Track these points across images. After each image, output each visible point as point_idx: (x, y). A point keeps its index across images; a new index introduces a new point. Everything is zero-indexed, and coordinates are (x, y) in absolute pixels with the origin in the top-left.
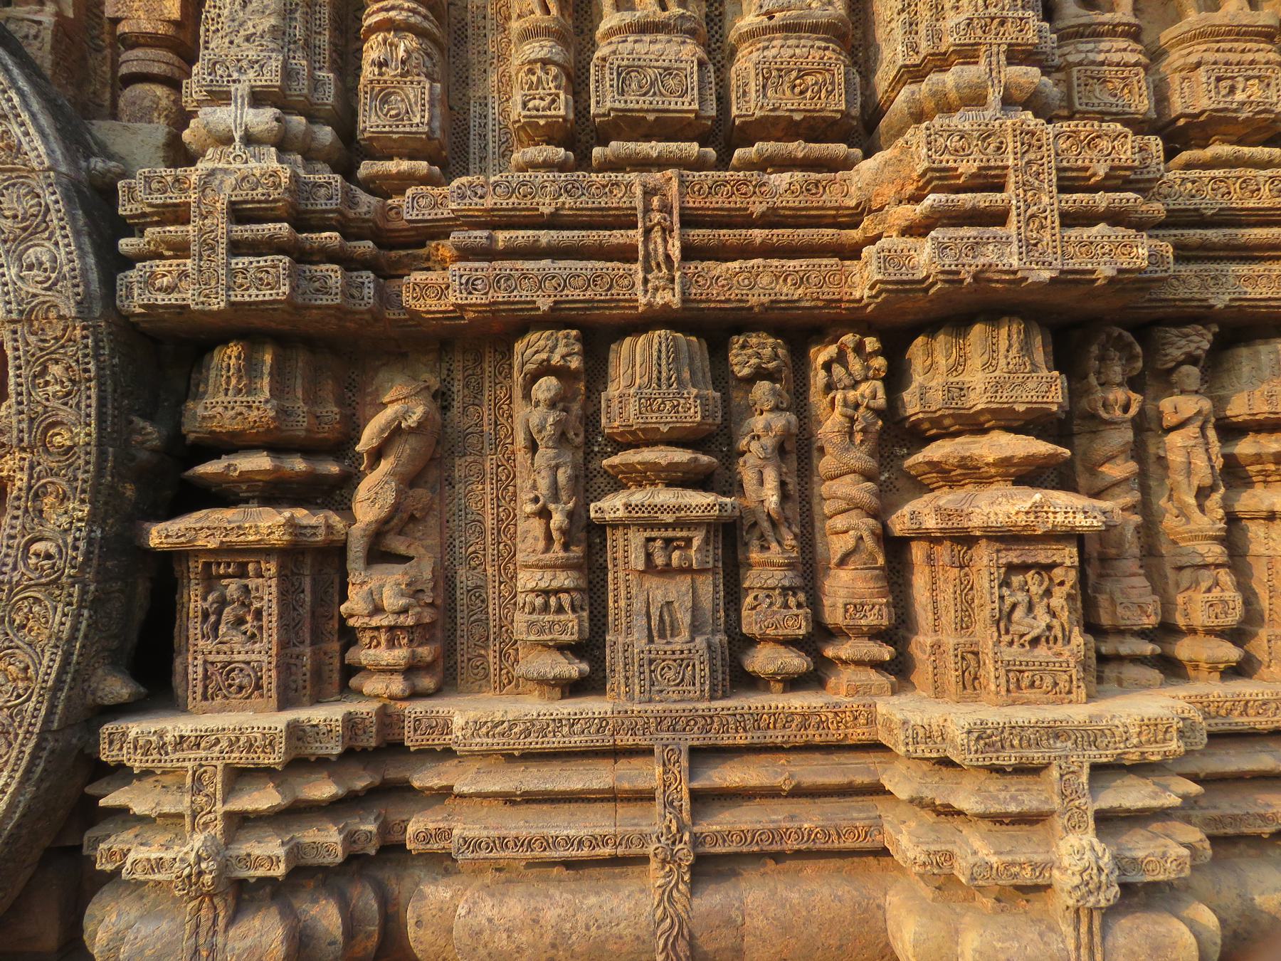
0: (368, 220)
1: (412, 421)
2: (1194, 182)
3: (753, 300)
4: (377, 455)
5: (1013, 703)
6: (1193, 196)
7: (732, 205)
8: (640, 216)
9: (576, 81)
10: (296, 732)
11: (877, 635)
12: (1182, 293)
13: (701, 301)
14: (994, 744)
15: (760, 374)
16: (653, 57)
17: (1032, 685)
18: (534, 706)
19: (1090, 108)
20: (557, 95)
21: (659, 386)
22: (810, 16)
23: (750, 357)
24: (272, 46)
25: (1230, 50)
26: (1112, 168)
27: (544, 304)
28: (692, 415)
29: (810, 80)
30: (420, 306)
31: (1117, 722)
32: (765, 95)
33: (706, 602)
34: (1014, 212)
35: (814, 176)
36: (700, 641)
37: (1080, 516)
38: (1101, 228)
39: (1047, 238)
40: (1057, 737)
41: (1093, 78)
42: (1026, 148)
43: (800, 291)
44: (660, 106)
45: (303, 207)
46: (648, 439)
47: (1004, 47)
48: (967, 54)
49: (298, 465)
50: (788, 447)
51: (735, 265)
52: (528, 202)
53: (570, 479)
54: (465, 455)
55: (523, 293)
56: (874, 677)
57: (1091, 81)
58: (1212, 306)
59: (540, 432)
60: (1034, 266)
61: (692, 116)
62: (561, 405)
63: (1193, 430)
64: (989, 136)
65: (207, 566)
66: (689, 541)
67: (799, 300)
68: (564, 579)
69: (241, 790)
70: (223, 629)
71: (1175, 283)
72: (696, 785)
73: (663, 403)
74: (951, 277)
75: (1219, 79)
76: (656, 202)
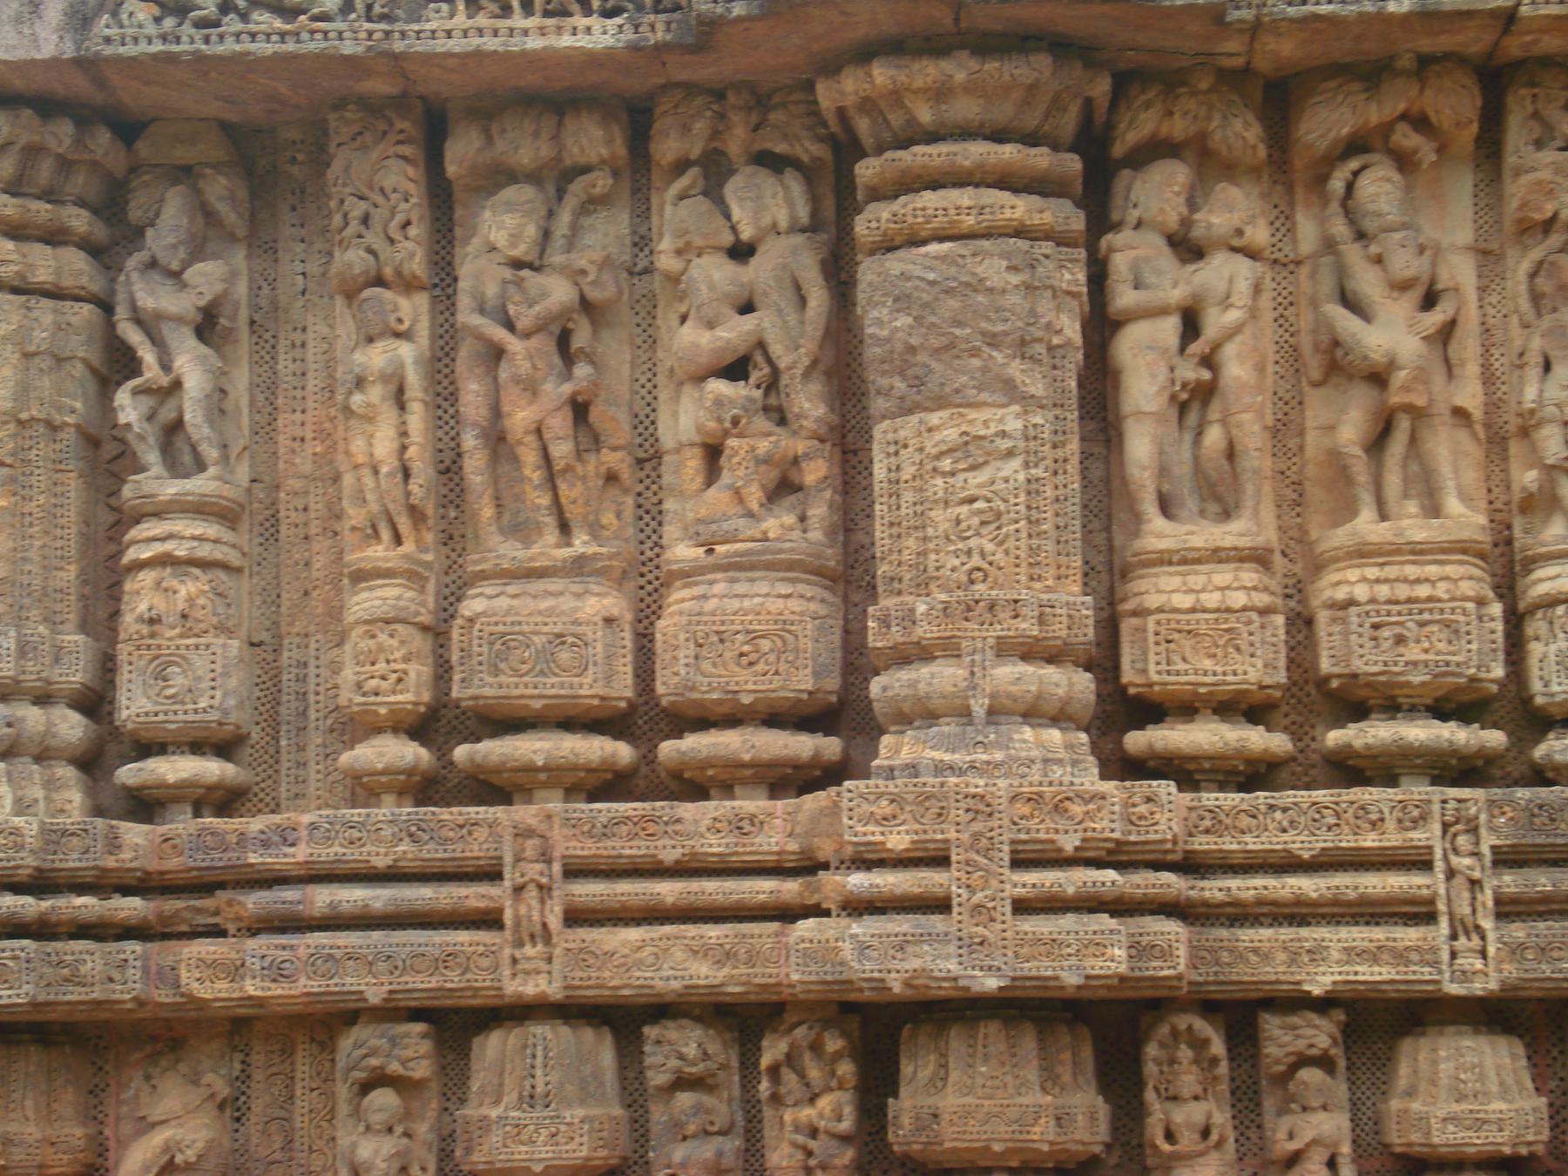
2: (1285, 810)
6: (1284, 831)
7: (634, 852)
12: (1267, 972)
20: (405, 672)
23: (667, 1057)
26: (1084, 840)
29: (765, 645)
30: (203, 992)
34: (955, 901)
38: (1068, 921)
41: (1179, 631)
42: (971, 815)
47: (991, 641)
48: (949, 649)
57: (1176, 636)
58: (1309, 992)
60: (977, 973)
64: (927, 798)
71: (1253, 958)
73: (536, 1131)
74: (874, 984)
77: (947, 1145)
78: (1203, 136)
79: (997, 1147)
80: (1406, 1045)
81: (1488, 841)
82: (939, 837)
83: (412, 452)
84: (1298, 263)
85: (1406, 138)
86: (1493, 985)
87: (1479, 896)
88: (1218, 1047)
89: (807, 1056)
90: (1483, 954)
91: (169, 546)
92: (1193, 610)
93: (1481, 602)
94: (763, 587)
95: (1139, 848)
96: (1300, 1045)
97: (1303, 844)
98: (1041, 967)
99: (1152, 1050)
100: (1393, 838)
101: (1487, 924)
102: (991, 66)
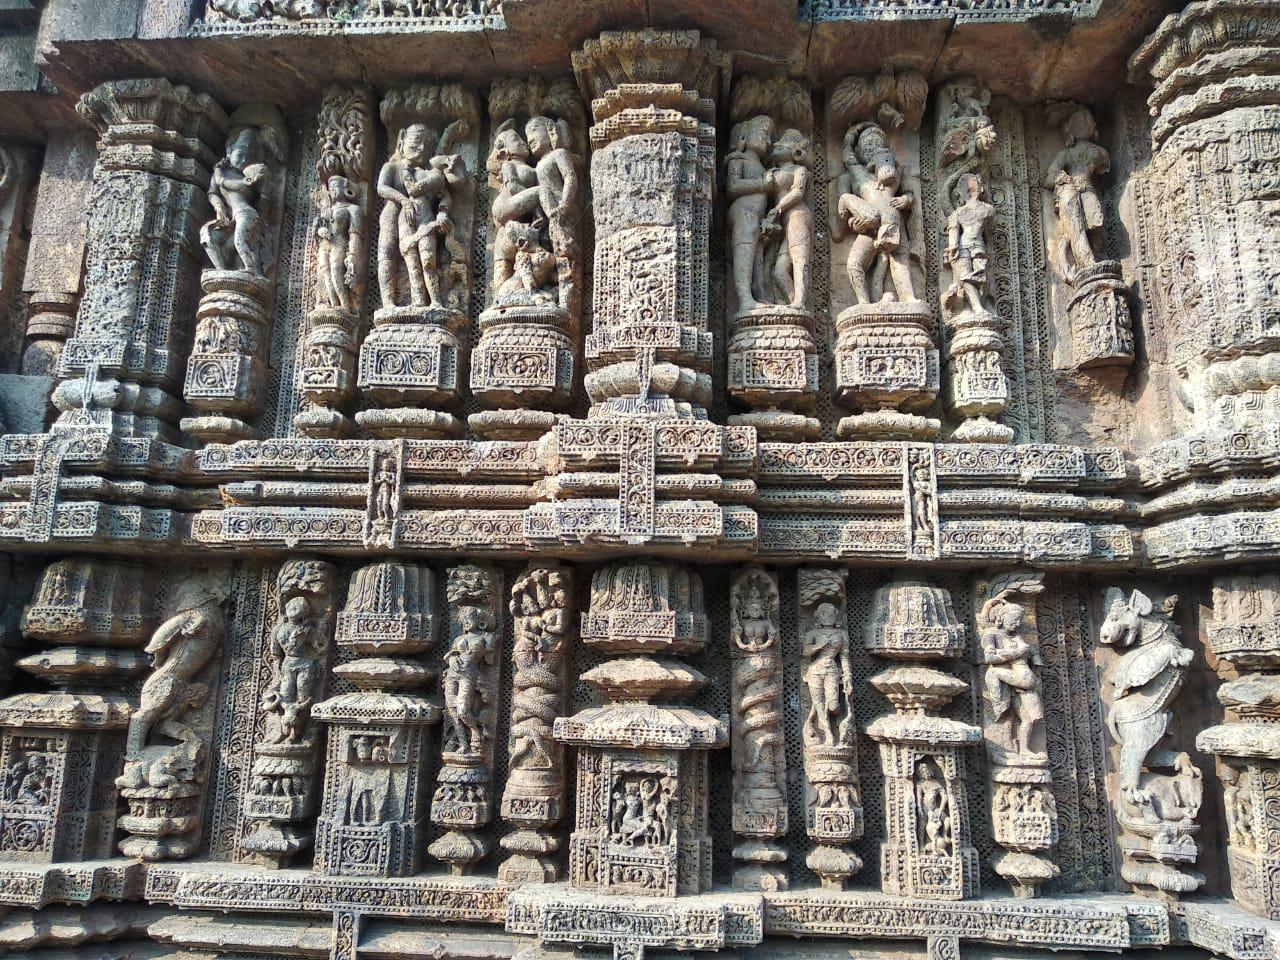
0: (170, 470)
1: (190, 629)
3: (454, 544)
4: (165, 654)
5: (614, 893)
7: (444, 467)
8: (370, 475)
9: (350, 356)
10: (54, 880)
11: (542, 829)
12: (804, 545)
13: (412, 543)
14: (566, 924)
15: (466, 600)
16: (406, 343)
17: (632, 878)
18: (264, 873)
19: (756, 385)
21: (376, 610)
22: (533, 312)
24: (121, 332)
25: (882, 335)
26: (700, 456)
27: (291, 542)
28: (399, 635)
29: (529, 361)
30: (203, 538)
31: (671, 912)
32: (492, 374)
33: (400, 792)
35: (511, 445)
36: (386, 827)
37: (668, 735)
38: (688, 504)
39: (644, 510)
40: (620, 921)
42: (633, 440)
43: (491, 537)
44: (408, 383)
45: (120, 463)
46: (364, 653)
48: (629, 355)
49: (100, 661)
50: (489, 660)
51: (442, 514)
52: (287, 462)
53: (306, 682)
54: (240, 656)
55: (275, 534)
56: (534, 865)
59: (284, 643)
60: (632, 532)
61: (434, 389)
62: (305, 622)
63: (825, 661)
65: (17, 740)
66: (387, 739)
67: (491, 544)
68: (287, 766)
69: (7, 925)
70: (21, 791)
71: (797, 536)
72: (363, 949)
75: (870, 360)
76: (384, 463)
77: (611, 638)
78: (780, 106)
79: (642, 640)
80: (881, 592)
81: (934, 473)
82: (613, 452)
83: (349, 258)
84: (828, 181)
85: (888, 111)
86: (937, 554)
87: (929, 502)
88: (774, 589)
89: (538, 587)
90: (932, 536)
91: (218, 305)
92: (769, 348)
93: (928, 348)
94: (530, 331)
95: (734, 465)
96: (822, 589)
97: (830, 472)
98: (669, 530)
99: (735, 590)
100: (880, 469)
101: (934, 519)
102: (666, 35)
